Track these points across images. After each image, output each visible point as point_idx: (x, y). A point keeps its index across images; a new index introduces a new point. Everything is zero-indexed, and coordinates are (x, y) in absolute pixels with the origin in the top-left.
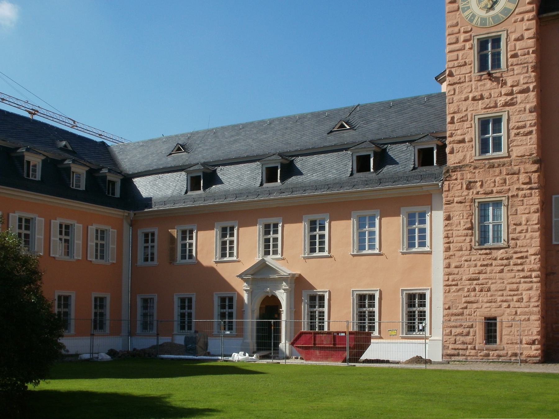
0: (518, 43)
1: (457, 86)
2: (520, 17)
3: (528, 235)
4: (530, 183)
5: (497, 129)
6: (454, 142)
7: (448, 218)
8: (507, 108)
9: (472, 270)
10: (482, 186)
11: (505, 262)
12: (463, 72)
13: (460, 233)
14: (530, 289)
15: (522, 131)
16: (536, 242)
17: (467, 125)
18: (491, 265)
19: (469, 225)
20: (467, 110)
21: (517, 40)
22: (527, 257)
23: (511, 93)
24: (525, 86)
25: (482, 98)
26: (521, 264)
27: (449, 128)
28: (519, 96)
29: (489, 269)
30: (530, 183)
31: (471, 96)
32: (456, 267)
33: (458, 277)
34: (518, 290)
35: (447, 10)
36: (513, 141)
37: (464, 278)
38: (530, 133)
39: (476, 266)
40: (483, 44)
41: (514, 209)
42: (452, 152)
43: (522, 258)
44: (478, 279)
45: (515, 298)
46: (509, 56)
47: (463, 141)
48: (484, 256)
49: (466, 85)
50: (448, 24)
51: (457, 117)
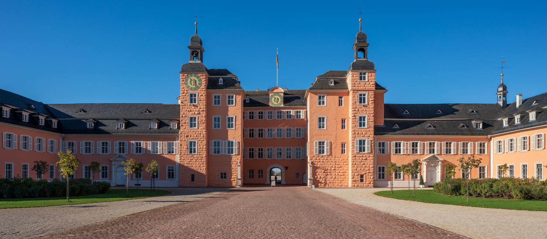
0: (201, 97)
1: (184, 107)
2: (201, 90)
3: (203, 152)
4: (204, 137)
5: (195, 121)
6: (182, 123)
7: (181, 145)
8: (198, 115)
9: (187, 160)
10: (190, 137)
11: (197, 159)
12: (185, 102)
13: (184, 150)
14: (204, 166)
15: (202, 122)
16: (205, 154)
17: (186, 118)
18: (193, 159)
19: (187, 148)
20: (186, 114)
21: (201, 96)
22: (203, 158)
23: (199, 111)
24: (203, 110)
25: (191, 111)
26: (201, 159)
27: (181, 119)
28: (201, 112)
29: (192, 160)
30: (204, 137)
31: (187, 110)
32: (183, 160)
33: (183, 162)
34: (200, 166)
35: (181, 83)
36: (199, 125)
37: (185, 163)
38: (204, 123)
39: (189, 159)
40: (191, 95)
41: (199, 144)
42: (182, 126)
43: (201, 158)
44: (189, 163)
45: (199, 169)
46: (199, 100)
47: (185, 123)
48: (191, 157)
49: (186, 106)
50: (181, 87)
51: (183, 115)
